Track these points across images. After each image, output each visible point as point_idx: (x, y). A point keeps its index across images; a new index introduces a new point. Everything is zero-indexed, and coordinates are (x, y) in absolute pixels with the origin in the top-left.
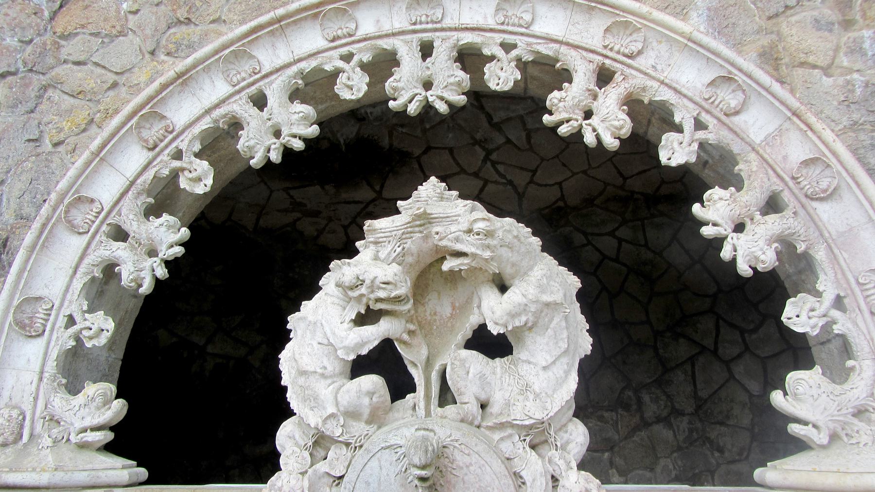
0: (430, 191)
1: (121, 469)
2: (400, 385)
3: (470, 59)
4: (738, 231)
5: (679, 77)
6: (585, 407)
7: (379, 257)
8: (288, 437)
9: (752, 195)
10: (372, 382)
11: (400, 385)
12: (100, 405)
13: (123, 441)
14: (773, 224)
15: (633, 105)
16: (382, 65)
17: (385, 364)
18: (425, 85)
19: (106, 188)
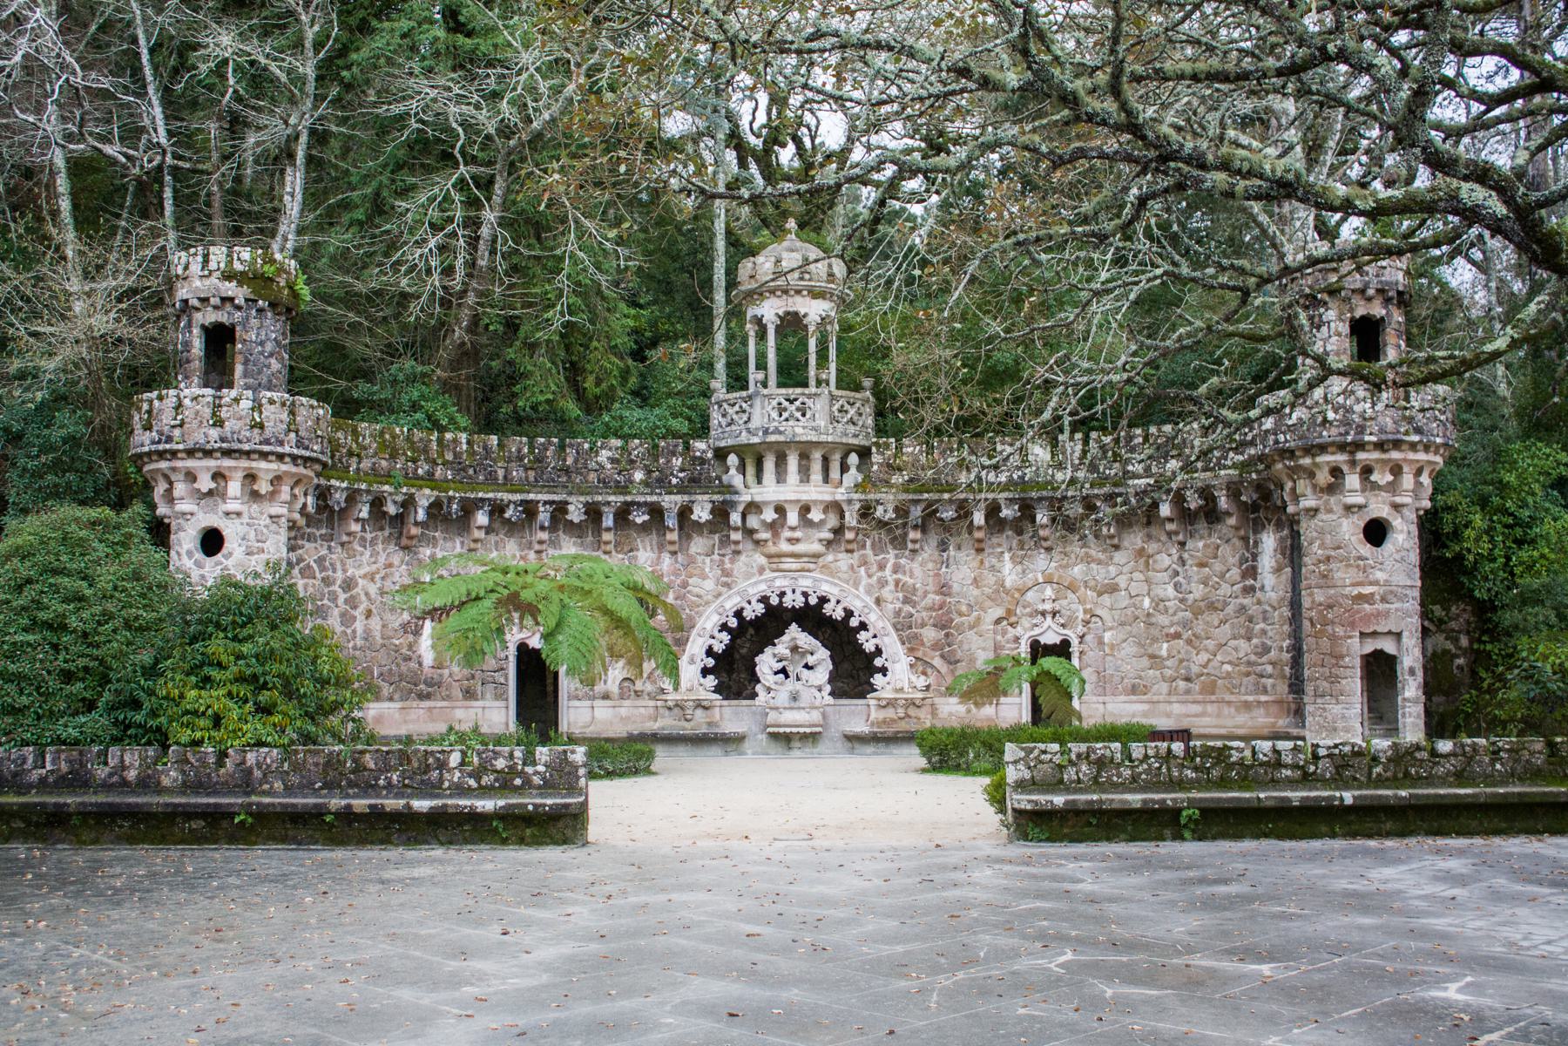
0: (794, 626)
1: (718, 696)
2: (787, 677)
3: (805, 594)
4: (867, 642)
5: (856, 605)
6: (830, 681)
7: (782, 647)
8: (758, 688)
9: (870, 634)
10: (782, 676)
11: (787, 677)
12: (711, 681)
13: (718, 690)
14: (875, 641)
15: (845, 609)
16: (782, 594)
17: (784, 671)
18: (793, 601)
19: (709, 626)
